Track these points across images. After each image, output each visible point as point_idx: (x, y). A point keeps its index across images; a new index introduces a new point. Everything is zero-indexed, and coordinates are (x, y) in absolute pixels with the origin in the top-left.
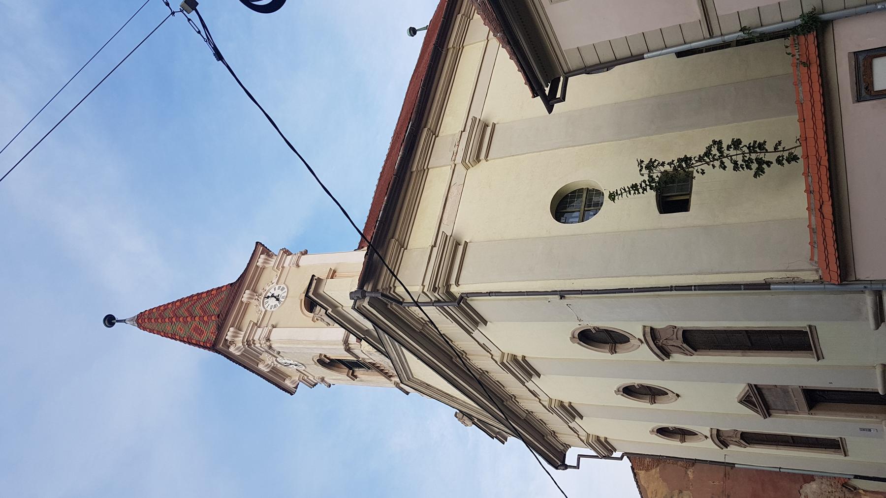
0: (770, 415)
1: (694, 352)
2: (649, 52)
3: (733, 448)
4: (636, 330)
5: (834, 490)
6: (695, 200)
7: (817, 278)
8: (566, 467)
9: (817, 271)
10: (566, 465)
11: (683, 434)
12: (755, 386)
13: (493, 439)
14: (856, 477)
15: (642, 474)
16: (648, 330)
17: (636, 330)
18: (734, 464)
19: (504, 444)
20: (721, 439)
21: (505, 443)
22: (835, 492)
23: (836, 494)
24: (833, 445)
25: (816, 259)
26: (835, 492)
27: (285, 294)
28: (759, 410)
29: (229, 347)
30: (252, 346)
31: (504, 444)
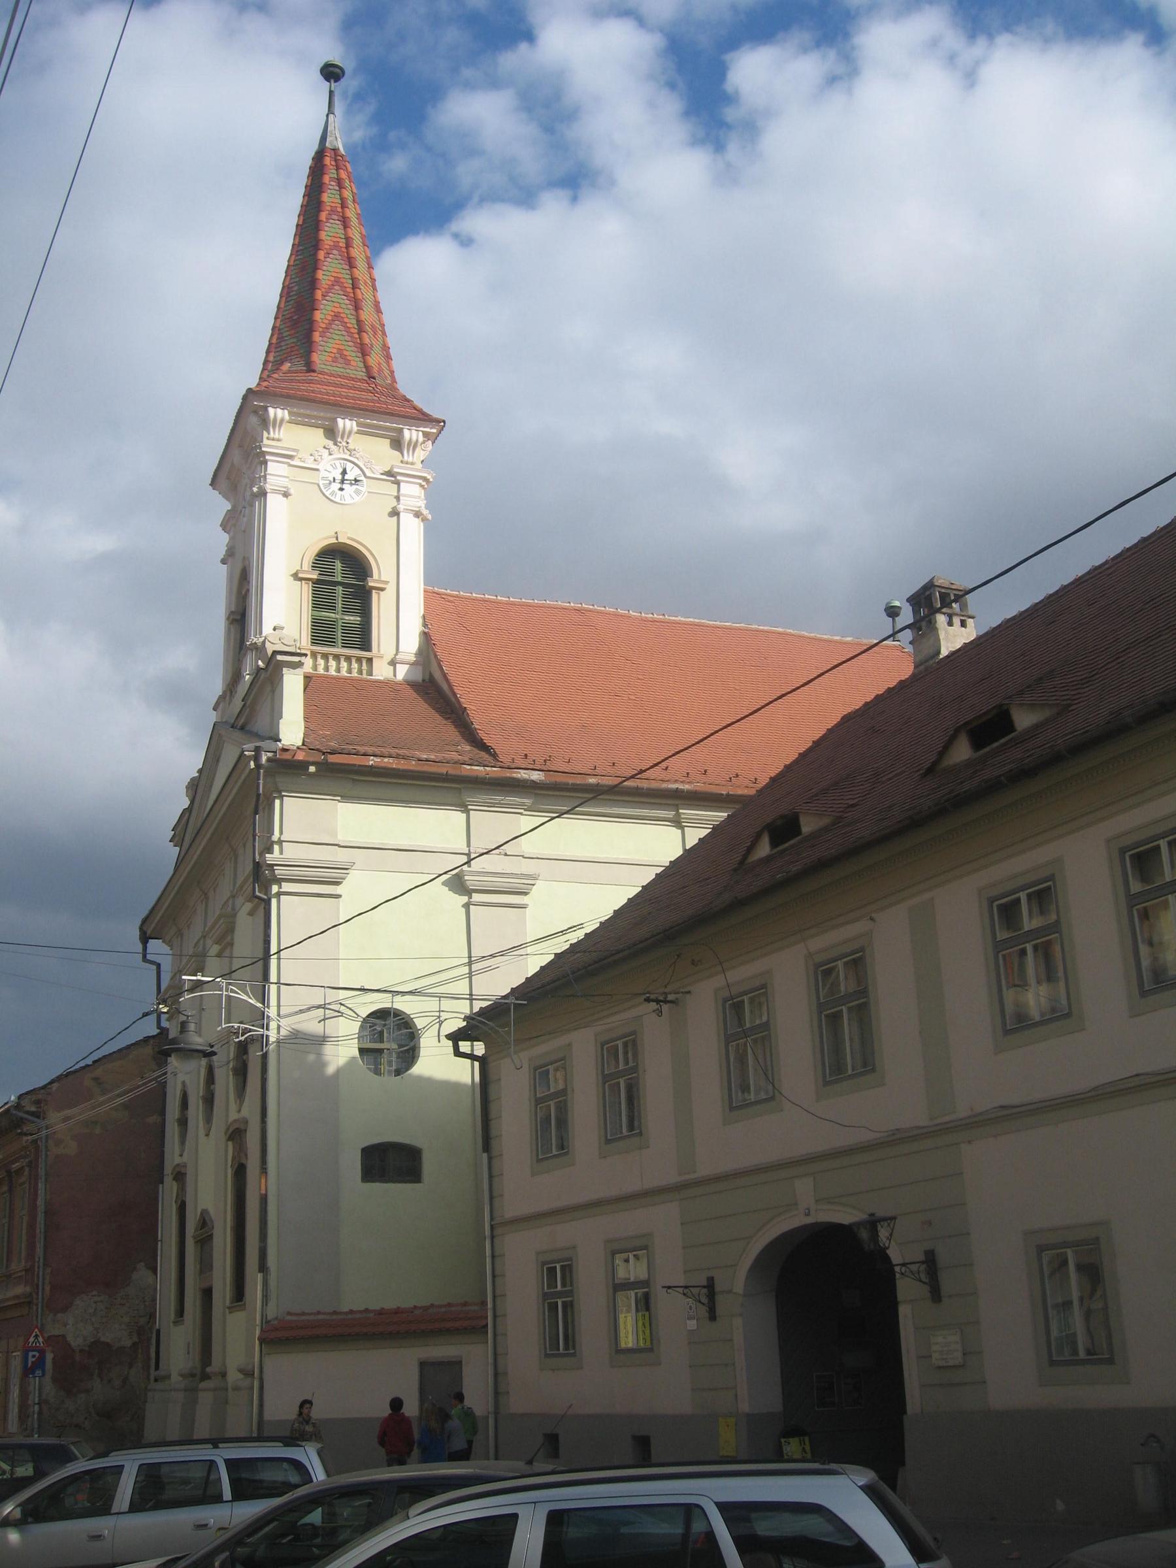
0: (196, 1242)
1: (234, 1170)
2: (490, 1159)
3: (175, 1185)
4: (245, 1112)
5: (147, 1303)
6: (377, 1187)
7: (269, 1318)
8: (145, 939)
9: (276, 1318)
10: (147, 942)
11: (183, 1122)
12: (212, 1234)
13: (173, 830)
14: (158, 1331)
15: (148, 1050)
16: (242, 1127)
17: (245, 1112)
18: (162, 1183)
19: (170, 841)
20: (180, 1176)
21: (172, 843)
22: (145, 1305)
23: (142, 1307)
24: (180, 1312)
25: (289, 1318)
26: (145, 1305)
27: (348, 501)
28: (198, 1232)
29: (255, 412)
30: (257, 460)
31: (170, 841)
